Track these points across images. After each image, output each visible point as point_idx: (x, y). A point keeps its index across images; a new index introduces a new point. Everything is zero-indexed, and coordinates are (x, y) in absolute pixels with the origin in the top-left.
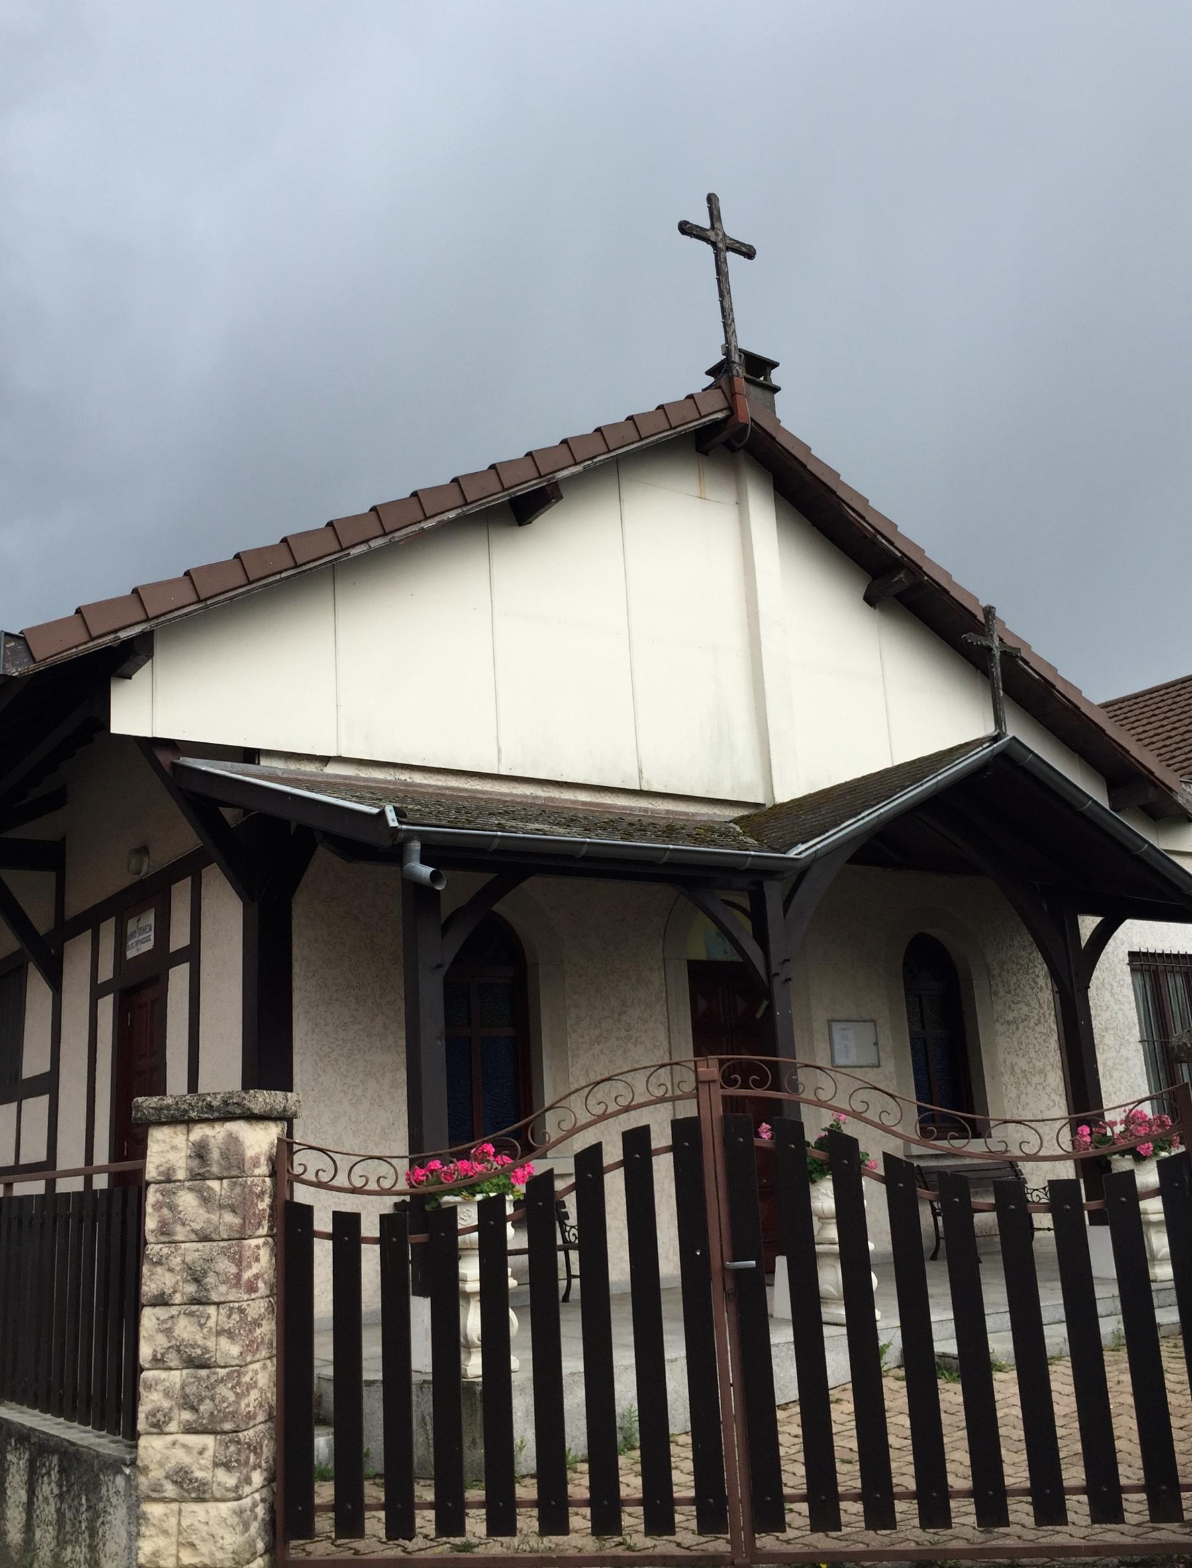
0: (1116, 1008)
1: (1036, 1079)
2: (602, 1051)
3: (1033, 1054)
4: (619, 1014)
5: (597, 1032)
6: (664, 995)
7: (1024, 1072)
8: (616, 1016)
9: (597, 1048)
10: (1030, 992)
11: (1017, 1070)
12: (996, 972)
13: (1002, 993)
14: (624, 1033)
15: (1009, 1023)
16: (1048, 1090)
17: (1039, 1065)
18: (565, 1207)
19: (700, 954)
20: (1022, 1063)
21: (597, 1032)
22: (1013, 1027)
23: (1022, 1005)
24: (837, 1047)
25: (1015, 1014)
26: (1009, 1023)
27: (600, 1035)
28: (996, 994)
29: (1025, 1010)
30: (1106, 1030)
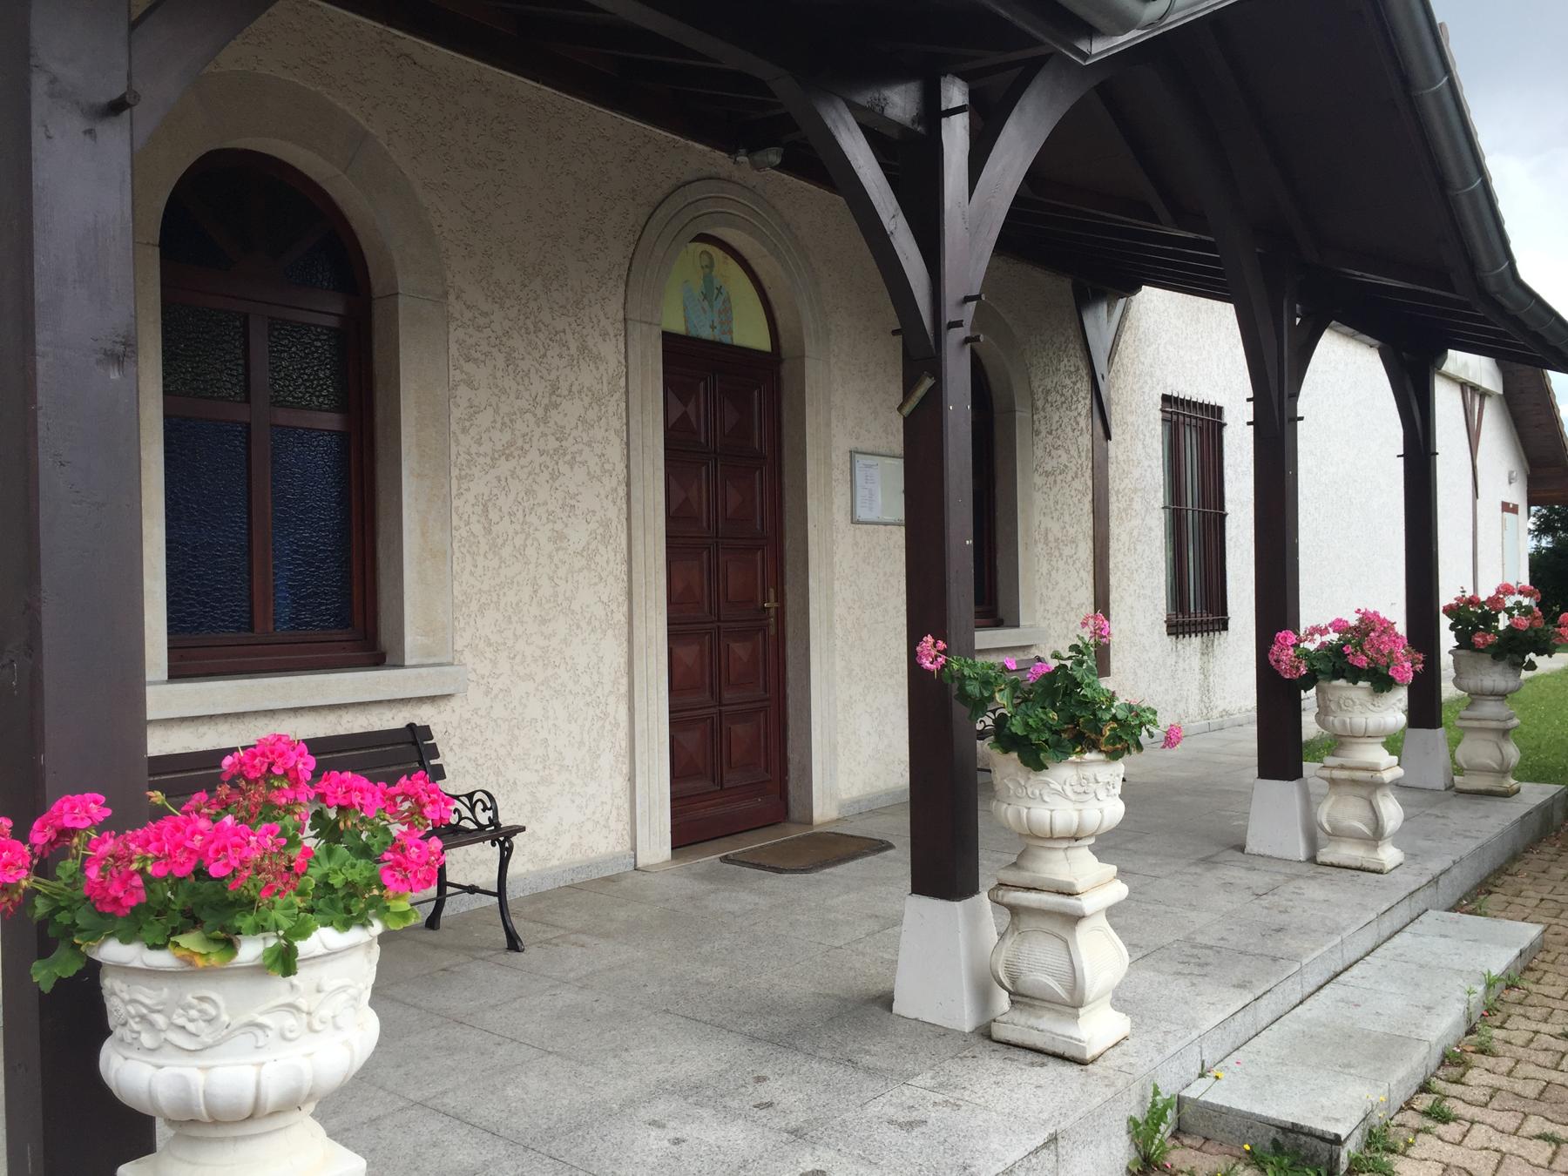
0: (1147, 463)
1: (1067, 551)
2: (513, 473)
3: (1067, 518)
4: (546, 409)
5: (507, 436)
6: (622, 382)
7: (1057, 540)
8: (540, 412)
9: (504, 466)
10: (1071, 434)
11: (1051, 538)
12: (1040, 404)
13: (1043, 434)
14: (553, 444)
15: (1047, 474)
16: (1078, 565)
17: (1072, 531)
18: (437, 756)
19: (677, 326)
20: (1055, 527)
21: (507, 436)
22: (1051, 479)
23: (1061, 452)
24: (861, 493)
25: (1054, 463)
26: (1047, 474)
27: (511, 444)
28: (1038, 433)
29: (1064, 458)
30: (1135, 491)
